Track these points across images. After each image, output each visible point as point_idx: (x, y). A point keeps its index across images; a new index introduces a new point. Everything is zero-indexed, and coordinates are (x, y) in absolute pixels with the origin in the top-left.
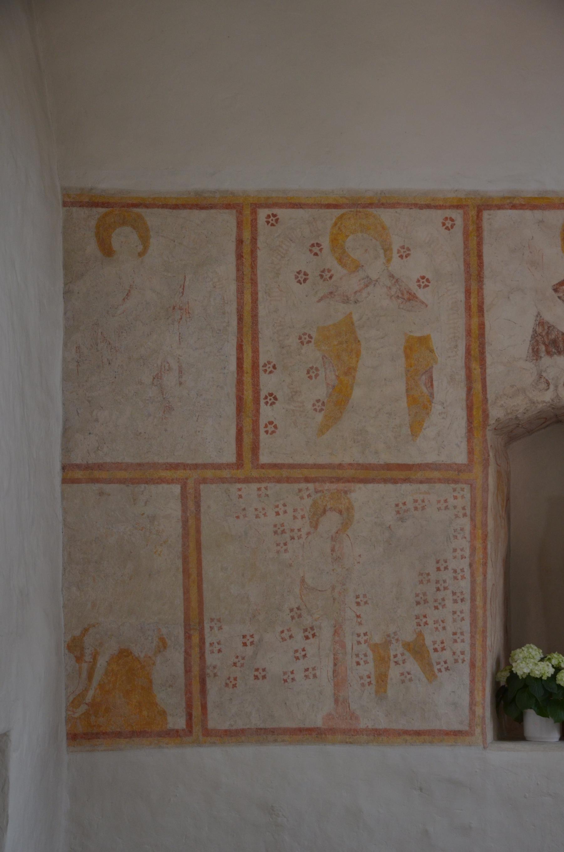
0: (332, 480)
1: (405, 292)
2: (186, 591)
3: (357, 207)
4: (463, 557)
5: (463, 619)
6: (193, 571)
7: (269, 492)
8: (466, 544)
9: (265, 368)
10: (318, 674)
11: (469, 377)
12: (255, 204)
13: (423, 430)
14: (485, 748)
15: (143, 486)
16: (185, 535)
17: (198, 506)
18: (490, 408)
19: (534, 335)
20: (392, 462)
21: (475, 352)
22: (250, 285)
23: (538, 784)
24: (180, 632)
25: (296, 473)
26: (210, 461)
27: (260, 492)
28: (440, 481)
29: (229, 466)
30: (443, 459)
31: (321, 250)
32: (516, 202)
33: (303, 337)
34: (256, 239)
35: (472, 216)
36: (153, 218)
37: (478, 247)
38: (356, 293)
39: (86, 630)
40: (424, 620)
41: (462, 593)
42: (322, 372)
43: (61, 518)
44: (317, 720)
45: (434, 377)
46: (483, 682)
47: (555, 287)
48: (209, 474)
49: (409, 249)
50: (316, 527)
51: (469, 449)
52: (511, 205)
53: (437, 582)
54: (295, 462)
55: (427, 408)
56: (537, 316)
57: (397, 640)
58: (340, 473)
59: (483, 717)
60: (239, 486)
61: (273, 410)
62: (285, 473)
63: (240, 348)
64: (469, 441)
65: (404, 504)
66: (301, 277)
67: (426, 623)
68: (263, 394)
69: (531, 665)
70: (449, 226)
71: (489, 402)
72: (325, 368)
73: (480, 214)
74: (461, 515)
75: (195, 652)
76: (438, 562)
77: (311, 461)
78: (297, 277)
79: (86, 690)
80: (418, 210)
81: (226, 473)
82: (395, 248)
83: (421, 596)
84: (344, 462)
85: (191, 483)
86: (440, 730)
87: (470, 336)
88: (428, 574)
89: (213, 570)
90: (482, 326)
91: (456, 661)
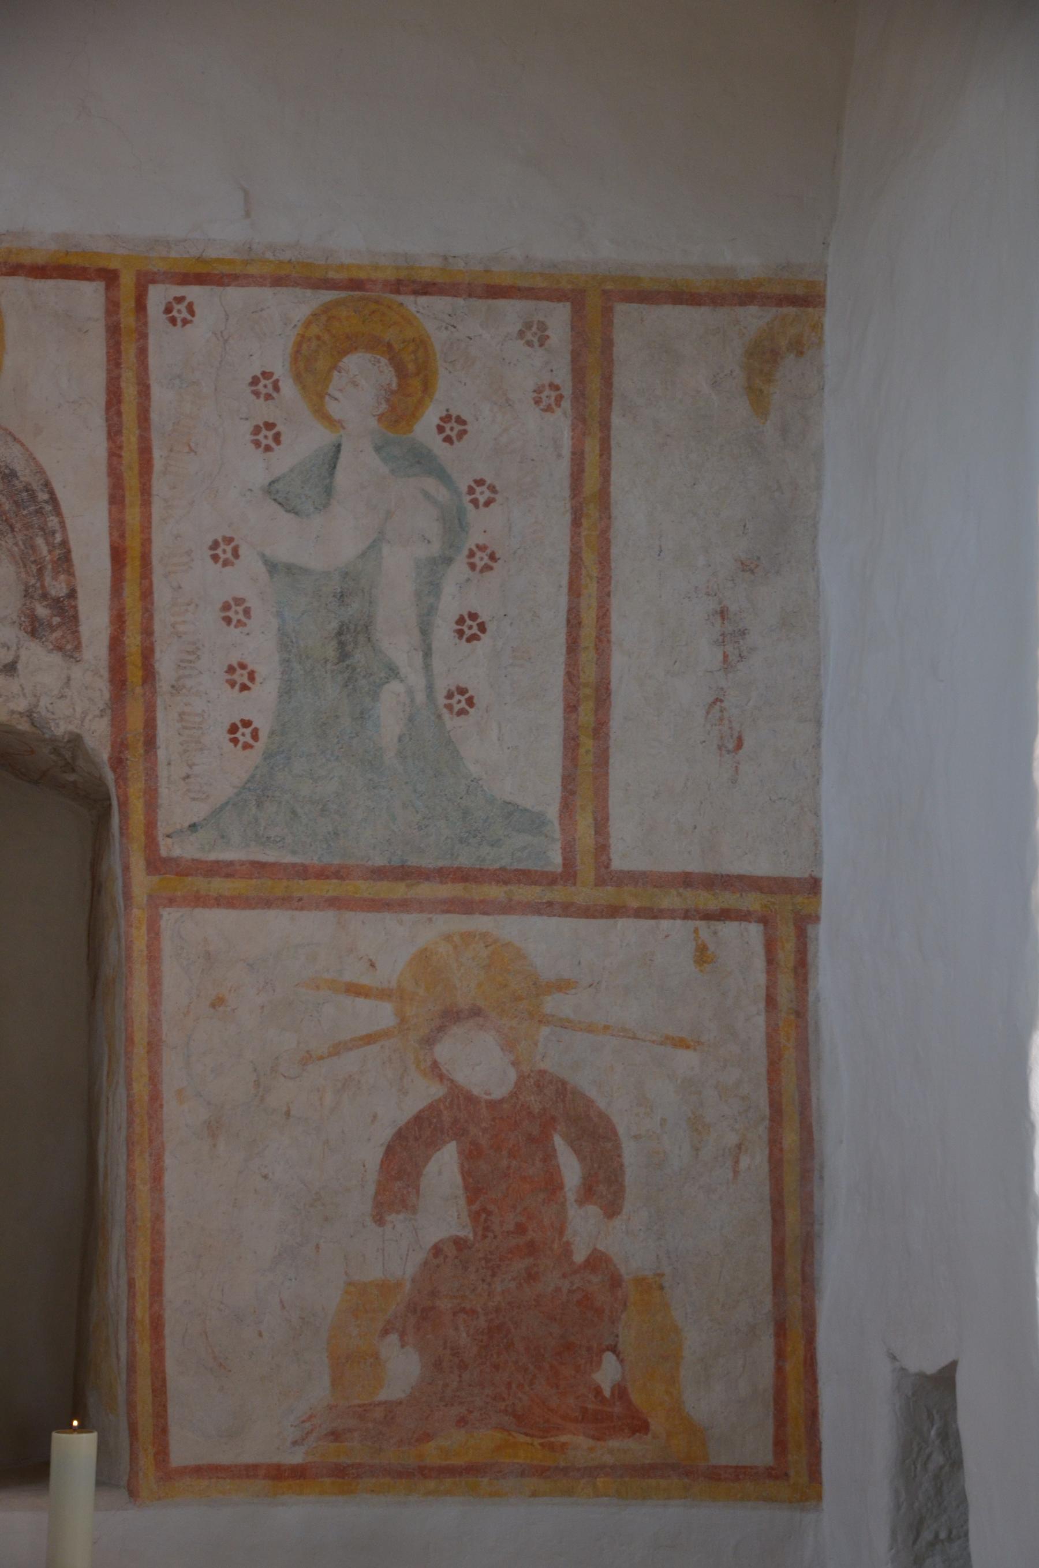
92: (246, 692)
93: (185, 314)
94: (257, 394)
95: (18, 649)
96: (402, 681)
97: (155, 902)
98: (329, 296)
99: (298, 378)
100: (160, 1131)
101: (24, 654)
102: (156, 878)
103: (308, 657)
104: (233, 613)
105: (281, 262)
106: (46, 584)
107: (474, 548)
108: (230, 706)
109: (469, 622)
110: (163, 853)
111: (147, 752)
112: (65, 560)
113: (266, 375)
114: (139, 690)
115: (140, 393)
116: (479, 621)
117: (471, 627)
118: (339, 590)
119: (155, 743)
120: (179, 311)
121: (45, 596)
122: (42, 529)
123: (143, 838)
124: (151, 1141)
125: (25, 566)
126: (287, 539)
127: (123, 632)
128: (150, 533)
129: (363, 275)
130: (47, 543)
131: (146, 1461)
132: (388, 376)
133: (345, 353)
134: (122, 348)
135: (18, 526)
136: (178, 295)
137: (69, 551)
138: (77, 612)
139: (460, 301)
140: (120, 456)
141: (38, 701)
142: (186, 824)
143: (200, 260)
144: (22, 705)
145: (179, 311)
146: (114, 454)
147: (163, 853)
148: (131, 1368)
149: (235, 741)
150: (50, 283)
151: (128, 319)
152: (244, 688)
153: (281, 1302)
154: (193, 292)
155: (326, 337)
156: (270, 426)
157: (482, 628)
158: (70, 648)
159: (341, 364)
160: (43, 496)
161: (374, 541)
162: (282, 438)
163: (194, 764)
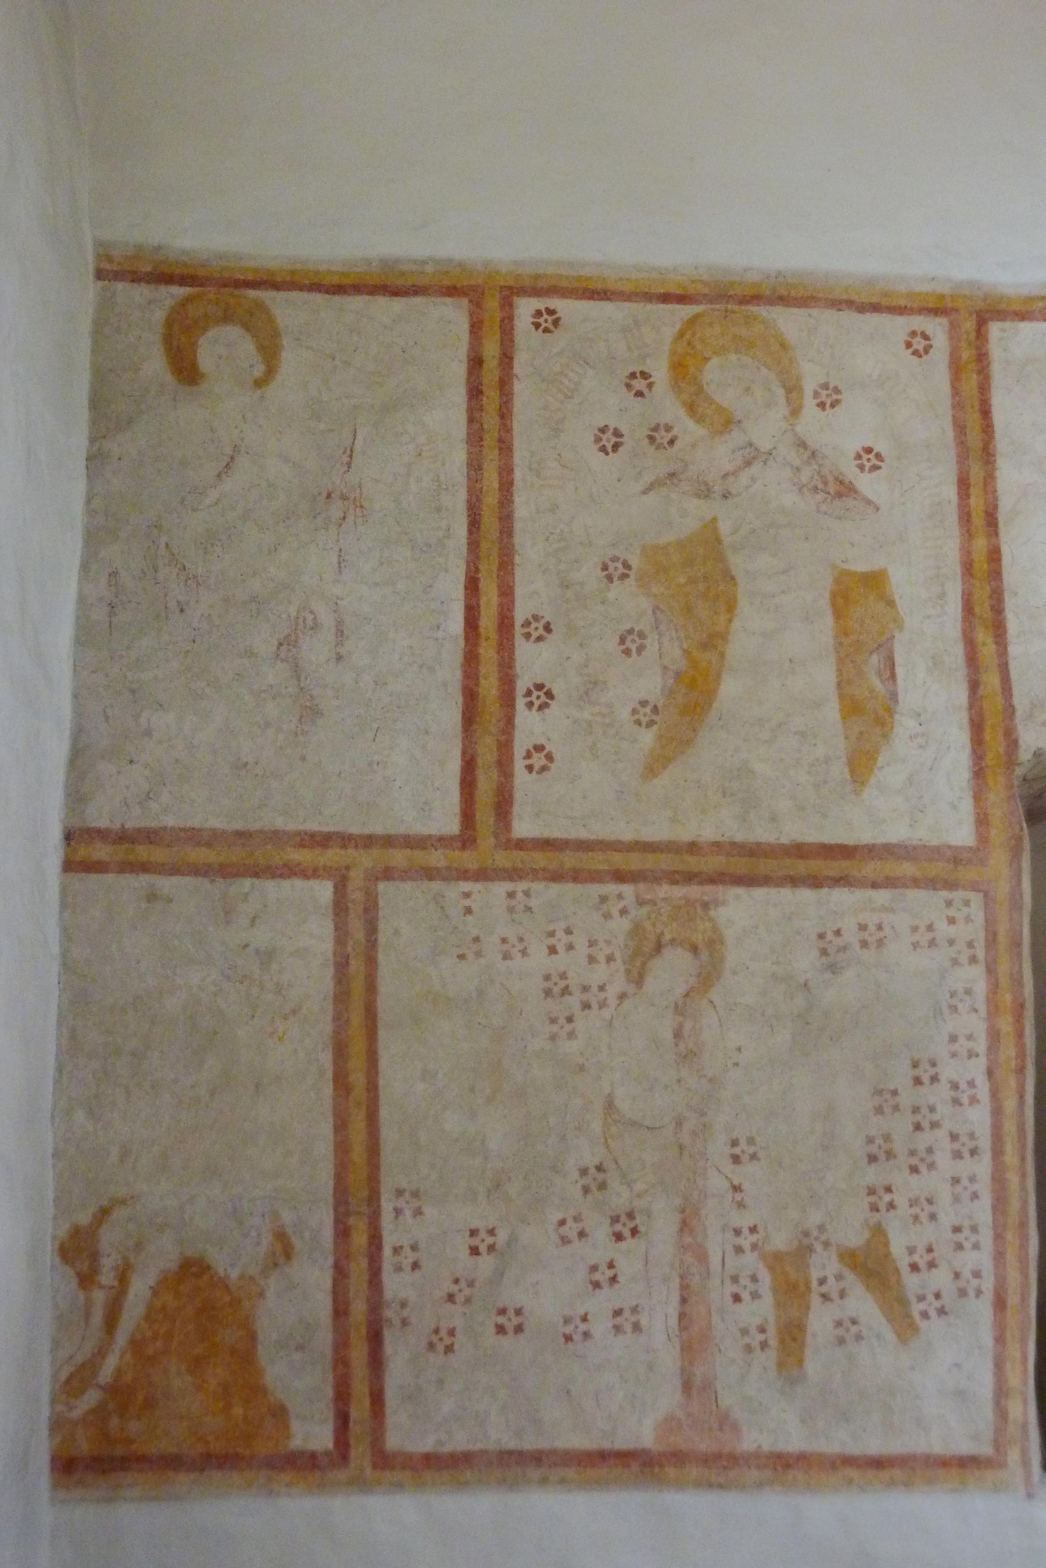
0: (676, 878)
1: (830, 478)
2: (341, 1126)
3: (727, 303)
4: (972, 1054)
5: (975, 1196)
6: (358, 1079)
7: (533, 903)
8: (978, 1026)
9: (527, 630)
10: (644, 1322)
12: (510, 288)
13: (876, 770)
14: (1030, 1496)
15: (247, 883)
16: (341, 997)
17: (372, 930)
20: (810, 839)
21: (983, 609)
22: (496, 452)
24: (324, 1220)
25: (598, 861)
26: (402, 830)
27: (513, 903)
28: (915, 883)
29: (443, 841)
30: (921, 834)
31: (650, 386)
33: (611, 566)
34: (511, 358)
36: (287, 310)
37: (982, 394)
38: (725, 476)
39: (104, 1212)
40: (887, 1198)
41: (972, 1136)
42: (652, 643)
43: (55, 949)
44: (642, 1432)
45: (899, 659)
46: (1024, 1341)
48: (399, 858)
49: (837, 390)
50: (639, 981)
51: (978, 814)
53: (916, 1110)
54: (593, 837)
57: (826, 1244)
58: (692, 863)
59: (1025, 1426)
60: (465, 886)
61: (544, 720)
62: (569, 860)
63: (472, 585)
65: (838, 933)
66: (608, 441)
67: (891, 1206)
68: (522, 685)
70: (921, 348)
71: (1019, 713)
72: (661, 635)
74: (964, 958)
75: (359, 1268)
76: (915, 1065)
77: (627, 835)
78: (598, 440)
79: (101, 1353)
80: (855, 316)
81: (437, 858)
82: (809, 386)
83: (879, 1141)
84: (700, 839)
85: (356, 879)
87: (971, 575)
88: (895, 1093)
89: (400, 1077)
90: (995, 556)
91: (963, 1293)
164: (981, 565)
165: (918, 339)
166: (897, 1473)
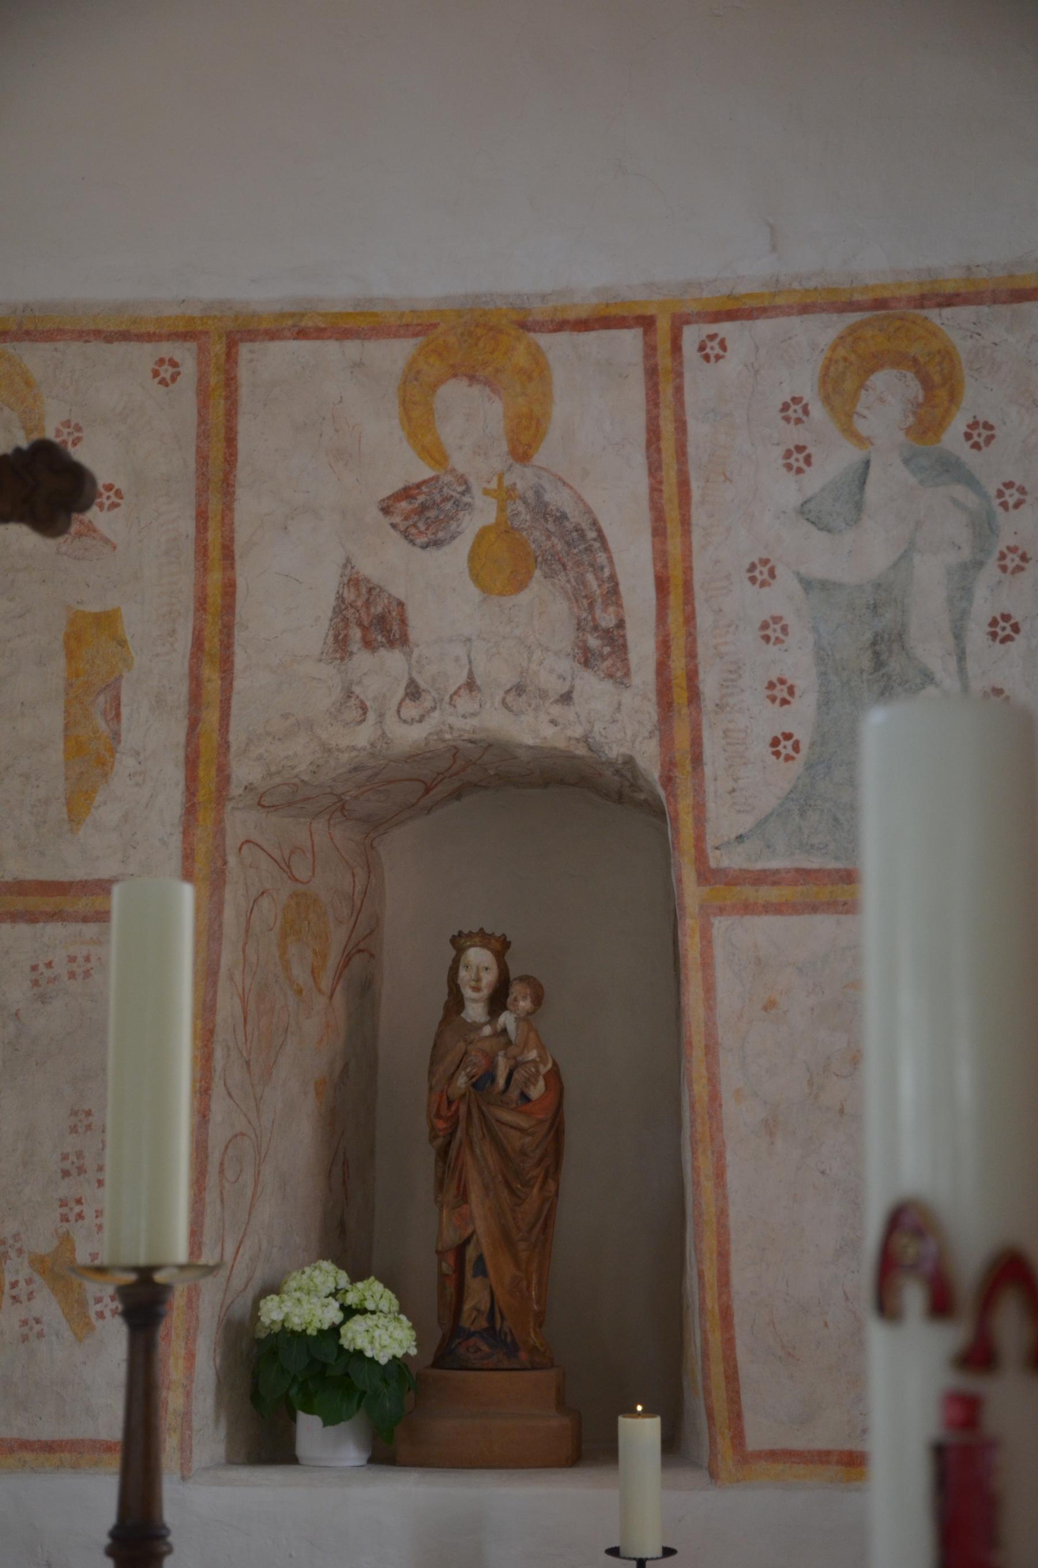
11: (195, 698)
13: (93, 810)
14: (183, 1478)
18: (233, 764)
19: (338, 606)
20: (29, 877)
23: (291, 1556)
32: (307, 323)
35: (216, 355)
37: (228, 421)
40: (77, 1209)
45: (124, 699)
46: (190, 1338)
47: (385, 505)
49: (79, 429)
51: (185, 849)
52: (296, 329)
55: (103, 764)
56: (345, 566)
57: (20, 1251)
64: (187, 832)
65: (49, 965)
67: (80, 1216)
69: (289, 1304)
71: (233, 749)
73: (234, 351)
80: (104, 346)
83: (73, 1158)
86: (95, 1441)
87: (204, 610)
88: (89, 1113)
90: (229, 589)
92: (786, 706)
93: (718, 351)
94: (787, 419)
95: (573, 679)
96: (937, 686)
97: (707, 912)
98: (854, 318)
99: (827, 400)
100: (720, 1130)
101: (578, 682)
102: (707, 889)
103: (844, 669)
104: (773, 630)
105: (807, 291)
106: (597, 617)
107: (1005, 551)
108: (769, 720)
109: (1002, 624)
110: (713, 864)
111: (694, 769)
112: (613, 594)
113: (796, 400)
114: (685, 711)
115: (676, 428)
116: (1013, 621)
117: (1004, 629)
118: (872, 602)
119: (701, 760)
120: (712, 348)
121: (596, 628)
122: (592, 565)
123: (693, 851)
124: (712, 1139)
125: (577, 601)
126: (821, 556)
127: (669, 657)
128: (691, 562)
129: (886, 294)
130: (597, 578)
131: (724, 1444)
132: (915, 389)
133: (872, 371)
134: (660, 388)
135: (569, 565)
136: (711, 332)
137: (617, 584)
138: (625, 640)
139: (985, 309)
140: (661, 491)
141: (593, 727)
142: (733, 836)
143: (730, 297)
144: (578, 731)
145: (712, 348)
146: (655, 489)
147: (713, 864)
148: (705, 1356)
149: (777, 754)
150: (593, 334)
151: (664, 361)
152: (784, 702)
153: (845, 1294)
154: (724, 329)
155: (853, 358)
156: (800, 449)
157: (1016, 628)
158: (620, 676)
159: (868, 383)
160: (592, 534)
161: (905, 551)
162: (813, 460)
163: (739, 778)
164: (215, 597)
165: (166, 366)
166: (66, 1456)
